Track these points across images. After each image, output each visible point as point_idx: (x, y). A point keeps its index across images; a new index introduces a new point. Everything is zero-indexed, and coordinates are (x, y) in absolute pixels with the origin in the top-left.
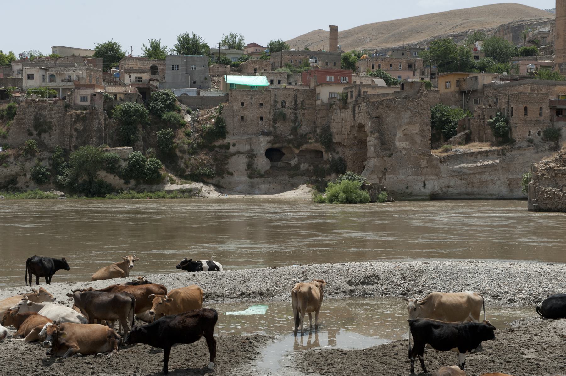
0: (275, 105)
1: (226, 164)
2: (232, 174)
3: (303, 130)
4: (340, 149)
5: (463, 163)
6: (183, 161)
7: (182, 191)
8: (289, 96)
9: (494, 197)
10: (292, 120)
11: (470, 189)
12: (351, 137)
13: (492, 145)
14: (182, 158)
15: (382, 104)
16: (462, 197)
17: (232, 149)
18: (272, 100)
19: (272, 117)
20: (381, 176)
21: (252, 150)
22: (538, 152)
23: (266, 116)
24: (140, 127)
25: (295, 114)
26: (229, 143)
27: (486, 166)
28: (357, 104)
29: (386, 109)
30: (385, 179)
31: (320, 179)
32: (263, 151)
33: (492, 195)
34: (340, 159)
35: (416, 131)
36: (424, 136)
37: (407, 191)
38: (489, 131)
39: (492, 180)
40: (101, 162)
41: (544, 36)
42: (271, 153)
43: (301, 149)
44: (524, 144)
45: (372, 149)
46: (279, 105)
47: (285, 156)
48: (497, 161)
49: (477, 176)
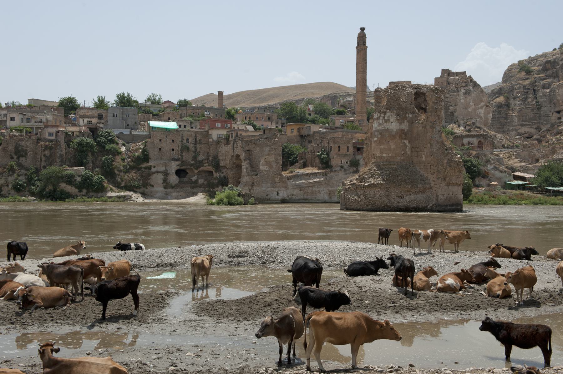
0: (182, 141)
1: (149, 179)
2: (153, 186)
3: (201, 157)
4: (224, 170)
5: (302, 180)
6: (120, 177)
7: (119, 197)
8: (191, 136)
9: (320, 201)
10: (193, 151)
11: (306, 197)
12: (232, 162)
13: (319, 169)
14: (119, 175)
15: (252, 142)
16: (301, 201)
17: (153, 170)
18: (180, 137)
20: (250, 188)
21: (167, 170)
22: (346, 174)
24: (90, 154)
25: (195, 147)
26: (151, 166)
27: (315, 182)
29: (254, 145)
30: (253, 190)
32: (174, 171)
33: (319, 200)
34: (225, 177)
36: (278, 163)
37: (267, 197)
38: (317, 160)
39: (319, 191)
40: (62, 177)
41: (350, 103)
42: (179, 173)
43: (199, 170)
44: (338, 169)
45: (245, 170)
46: (185, 141)
47: (188, 174)
48: (322, 179)
49: (310, 188)
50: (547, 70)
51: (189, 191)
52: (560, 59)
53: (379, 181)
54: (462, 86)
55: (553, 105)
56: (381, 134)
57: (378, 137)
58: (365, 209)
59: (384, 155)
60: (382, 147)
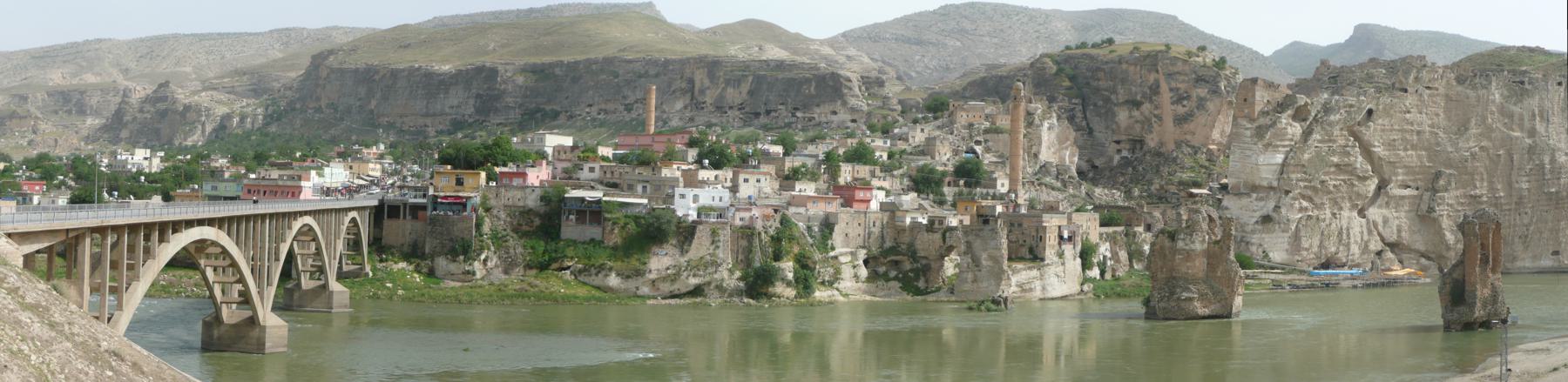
12: (938, 254)
23: (862, 233)
29: (974, 237)
55: (1110, 132)
56: (1188, 253)
59: (1190, 271)
60: (1188, 264)
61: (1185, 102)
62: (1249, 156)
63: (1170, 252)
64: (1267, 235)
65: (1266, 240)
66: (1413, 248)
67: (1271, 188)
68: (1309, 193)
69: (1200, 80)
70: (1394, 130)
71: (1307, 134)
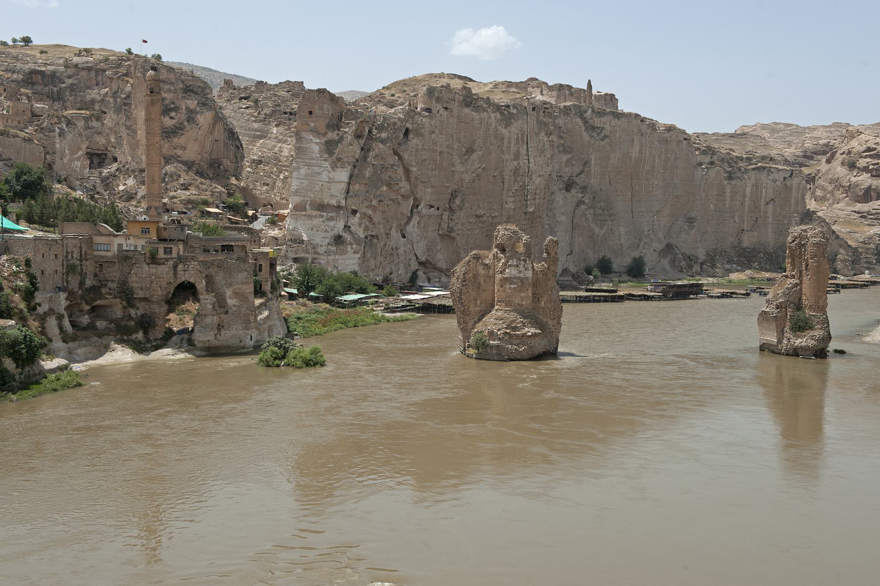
0: (67, 257)
12: (164, 293)
19: (65, 271)
28: (181, 262)
29: (216, 269)
30: (220, 335)
31: (125, 338)
34: (143, 316)
35: (249, 291)
37: (241, 344)
45: (210, 307)
50: (33, 84)
51: (99, 343)
52: (65, 74)
53: (533, 330)
54: (55, 123)
56: (521, 281)
57: (517, 284)
58: (526, 358)
59: (524, 303)
60: (522, 294)
61: (173, 114)
62: (319, 174)
63: (485, 281)
64: (340, 257)
65: (340, 262)
66: (437, 267)
67: (339, 207)
68: (370, 212)
69: (188, 90)
70: (425, 149)
71: (365, 150)
